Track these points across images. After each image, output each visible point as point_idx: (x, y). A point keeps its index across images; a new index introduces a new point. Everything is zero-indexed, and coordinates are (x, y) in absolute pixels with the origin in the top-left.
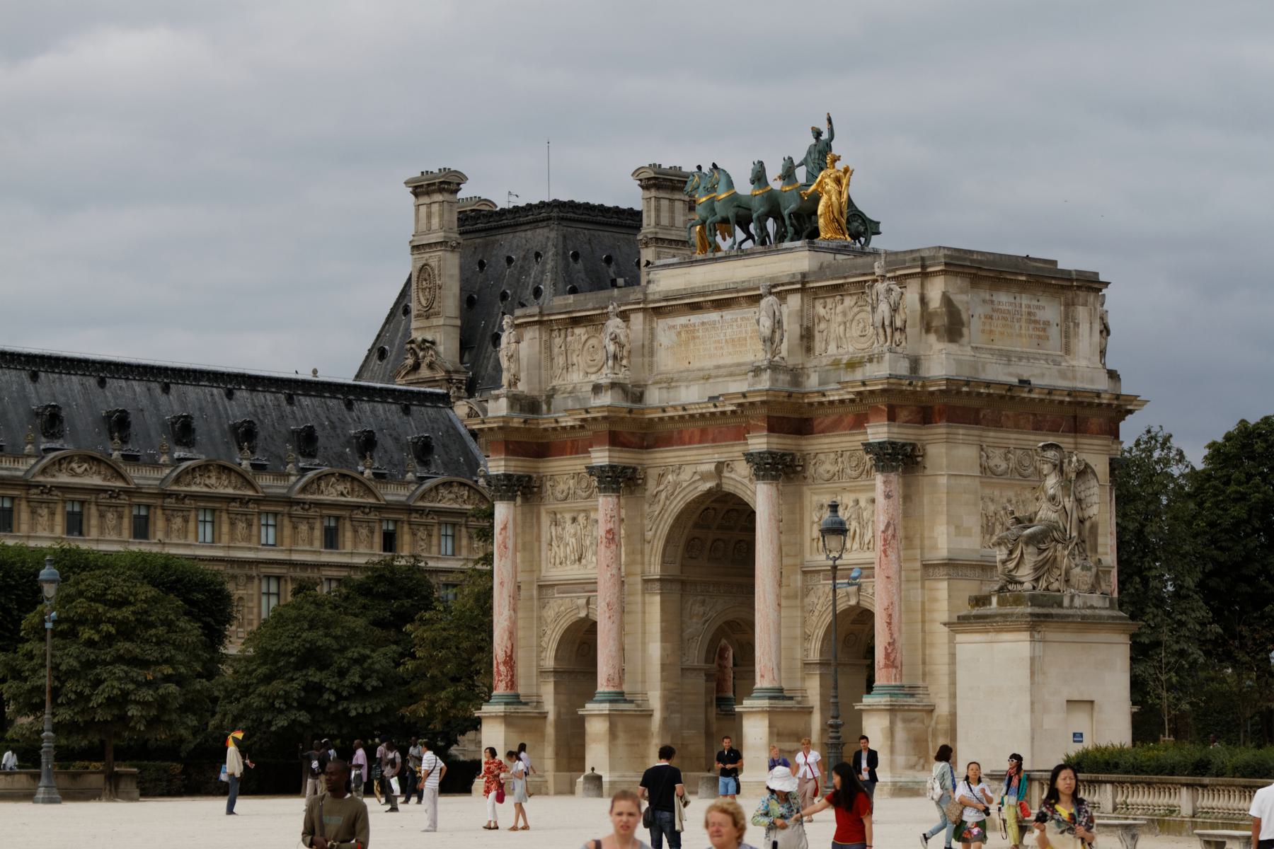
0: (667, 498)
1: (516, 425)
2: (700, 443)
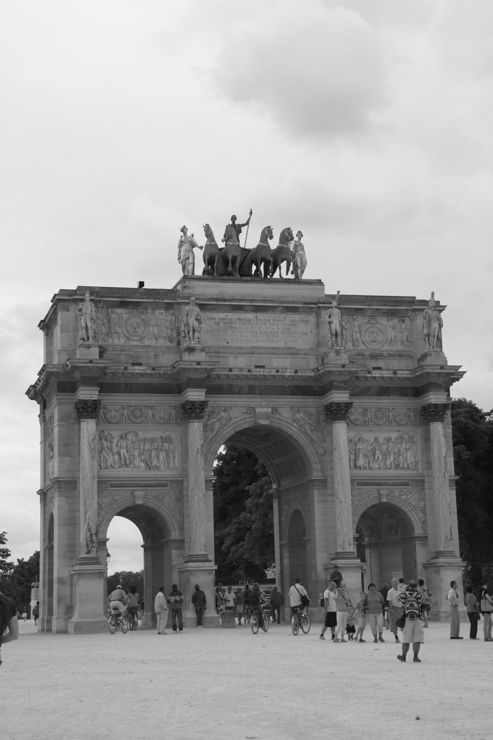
2: (248, 394)
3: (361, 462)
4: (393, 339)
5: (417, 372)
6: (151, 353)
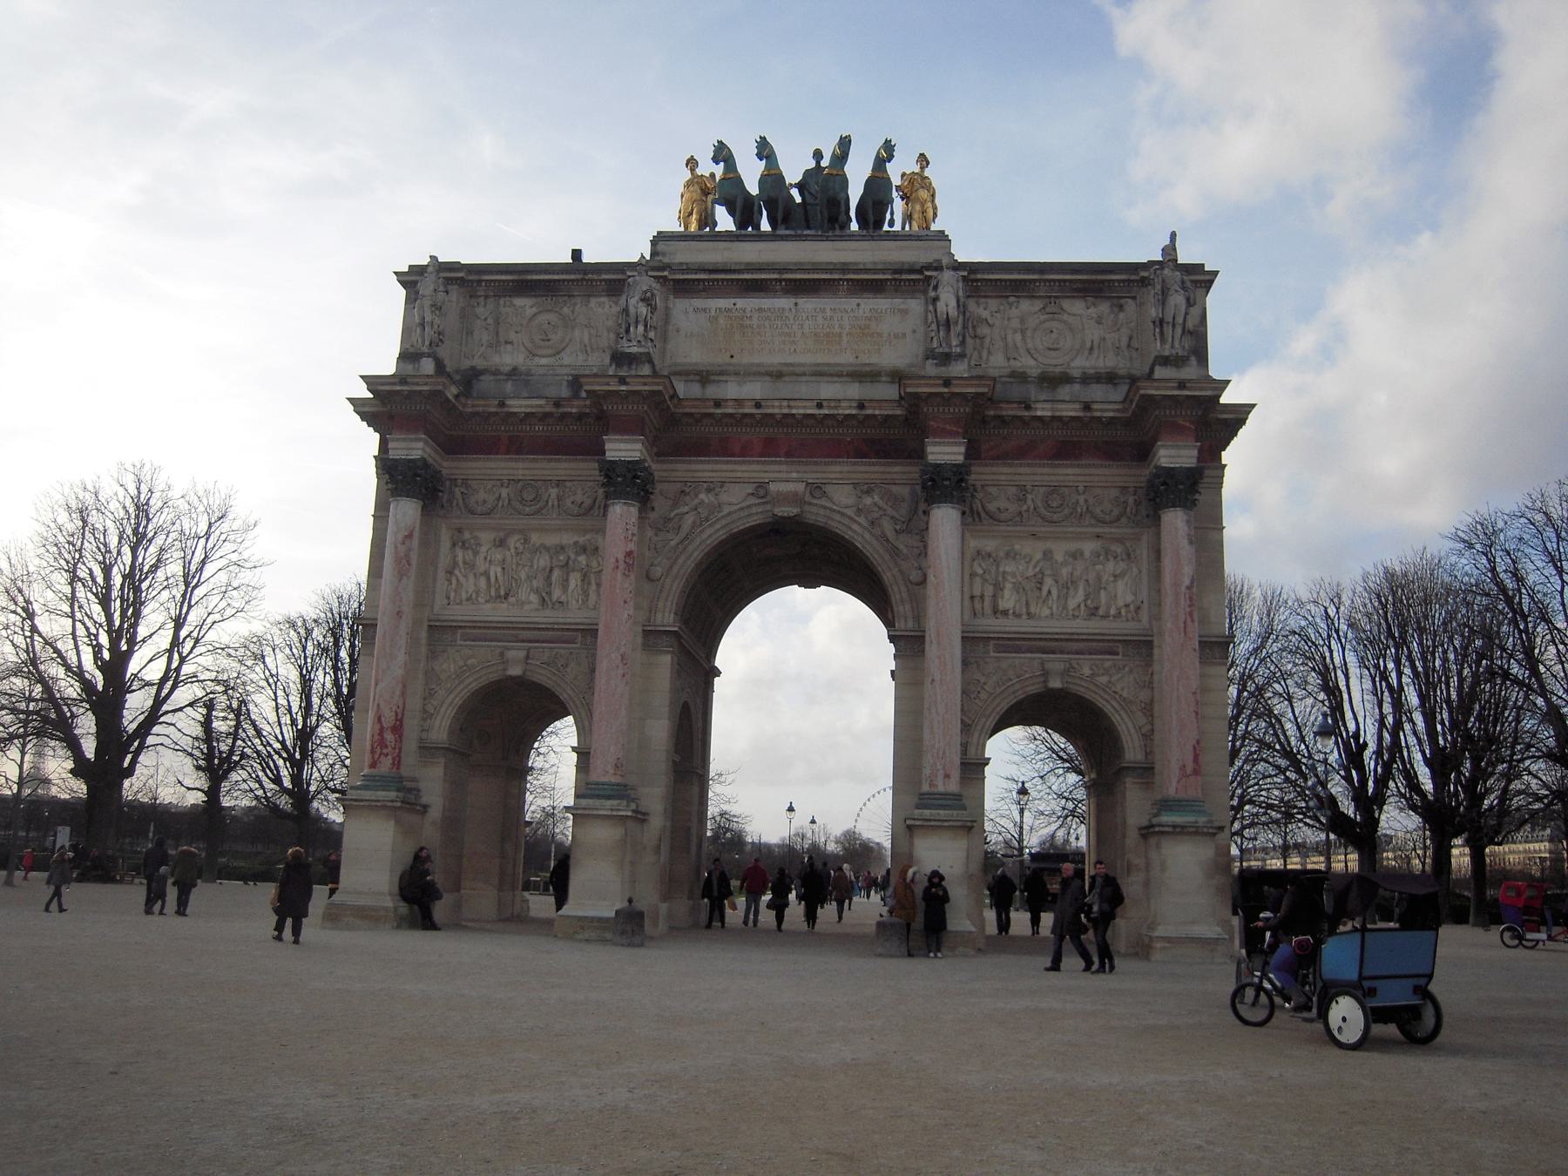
0: (694, 525)
1: (451, 397)
3: (1008, 600)
4: (1096, 343)
5: (1132, 401)
6: (566, 378)
